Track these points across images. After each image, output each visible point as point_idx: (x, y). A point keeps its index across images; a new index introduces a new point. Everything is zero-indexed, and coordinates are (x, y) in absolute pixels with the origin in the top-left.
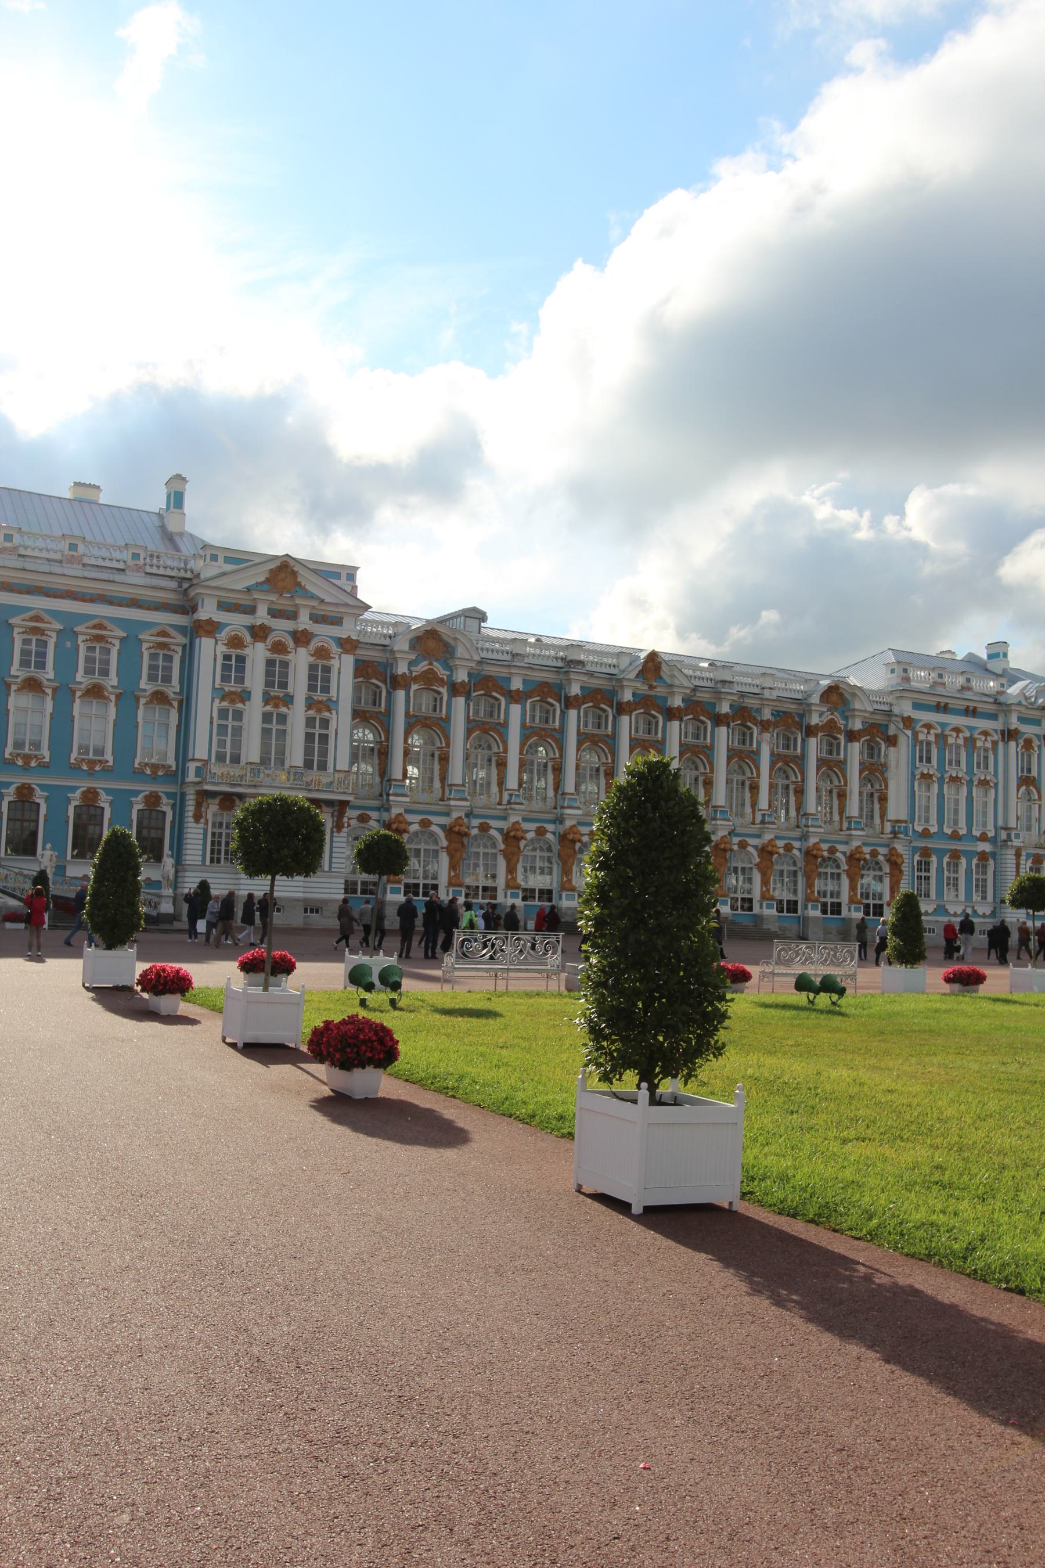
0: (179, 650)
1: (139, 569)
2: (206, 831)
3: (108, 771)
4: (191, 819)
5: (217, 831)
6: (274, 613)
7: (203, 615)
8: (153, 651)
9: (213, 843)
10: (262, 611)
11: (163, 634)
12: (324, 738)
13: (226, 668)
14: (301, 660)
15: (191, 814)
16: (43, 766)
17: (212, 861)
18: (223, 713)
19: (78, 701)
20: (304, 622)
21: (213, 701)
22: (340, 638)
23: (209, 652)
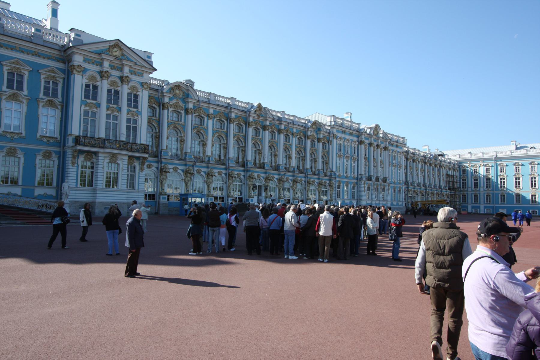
0: (61, 80)
3: (22, 139)
4: (70, 165)
6: (112, 67)
8: (47, 80)
9: (81, 176)
11: (53, 71)
12: (135, 129)
13: (87, 91)
15: (70, 162)
17: (81, 184)
18: (86, 113)
21: (81, 106)
23: (79, 82)
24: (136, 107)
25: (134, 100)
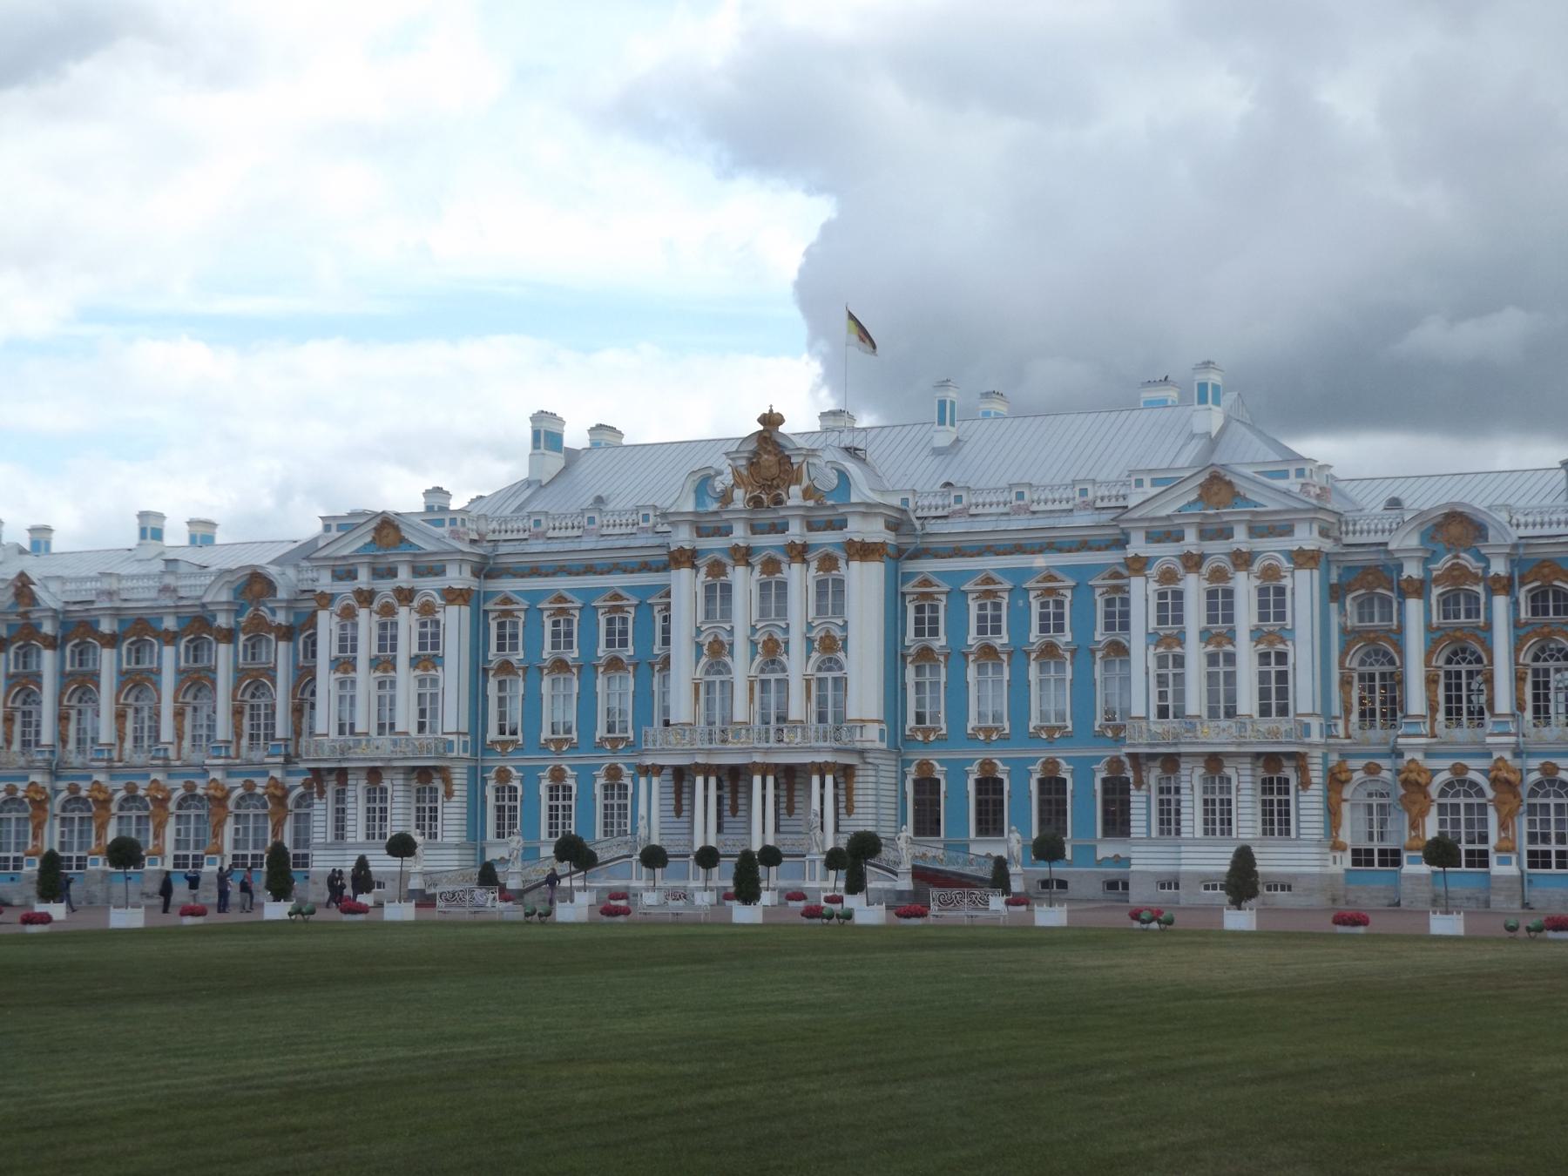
1: (1086, 506)
2: (1149, 798)
5: (1165, 797)
7: (1131, 551)
8: (1107, 596)
10: (1191, 537)
11: (1117, 575)
12: (1282, 677)
13: (1161, 607)
14: (1245, 586)
16: (1004, 738)
18: (1162, 661)
19: (1033, 664)
20: (1241, 539)
22: (1292, 552)
24: (1281, 616)
25: (1273, 600)
